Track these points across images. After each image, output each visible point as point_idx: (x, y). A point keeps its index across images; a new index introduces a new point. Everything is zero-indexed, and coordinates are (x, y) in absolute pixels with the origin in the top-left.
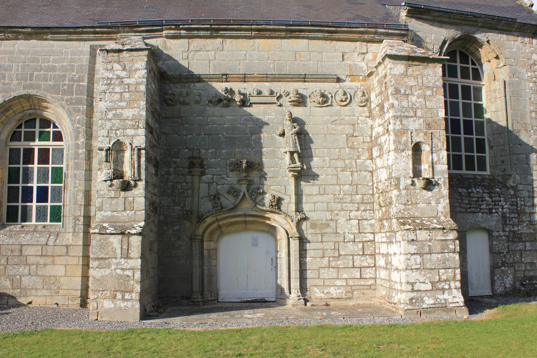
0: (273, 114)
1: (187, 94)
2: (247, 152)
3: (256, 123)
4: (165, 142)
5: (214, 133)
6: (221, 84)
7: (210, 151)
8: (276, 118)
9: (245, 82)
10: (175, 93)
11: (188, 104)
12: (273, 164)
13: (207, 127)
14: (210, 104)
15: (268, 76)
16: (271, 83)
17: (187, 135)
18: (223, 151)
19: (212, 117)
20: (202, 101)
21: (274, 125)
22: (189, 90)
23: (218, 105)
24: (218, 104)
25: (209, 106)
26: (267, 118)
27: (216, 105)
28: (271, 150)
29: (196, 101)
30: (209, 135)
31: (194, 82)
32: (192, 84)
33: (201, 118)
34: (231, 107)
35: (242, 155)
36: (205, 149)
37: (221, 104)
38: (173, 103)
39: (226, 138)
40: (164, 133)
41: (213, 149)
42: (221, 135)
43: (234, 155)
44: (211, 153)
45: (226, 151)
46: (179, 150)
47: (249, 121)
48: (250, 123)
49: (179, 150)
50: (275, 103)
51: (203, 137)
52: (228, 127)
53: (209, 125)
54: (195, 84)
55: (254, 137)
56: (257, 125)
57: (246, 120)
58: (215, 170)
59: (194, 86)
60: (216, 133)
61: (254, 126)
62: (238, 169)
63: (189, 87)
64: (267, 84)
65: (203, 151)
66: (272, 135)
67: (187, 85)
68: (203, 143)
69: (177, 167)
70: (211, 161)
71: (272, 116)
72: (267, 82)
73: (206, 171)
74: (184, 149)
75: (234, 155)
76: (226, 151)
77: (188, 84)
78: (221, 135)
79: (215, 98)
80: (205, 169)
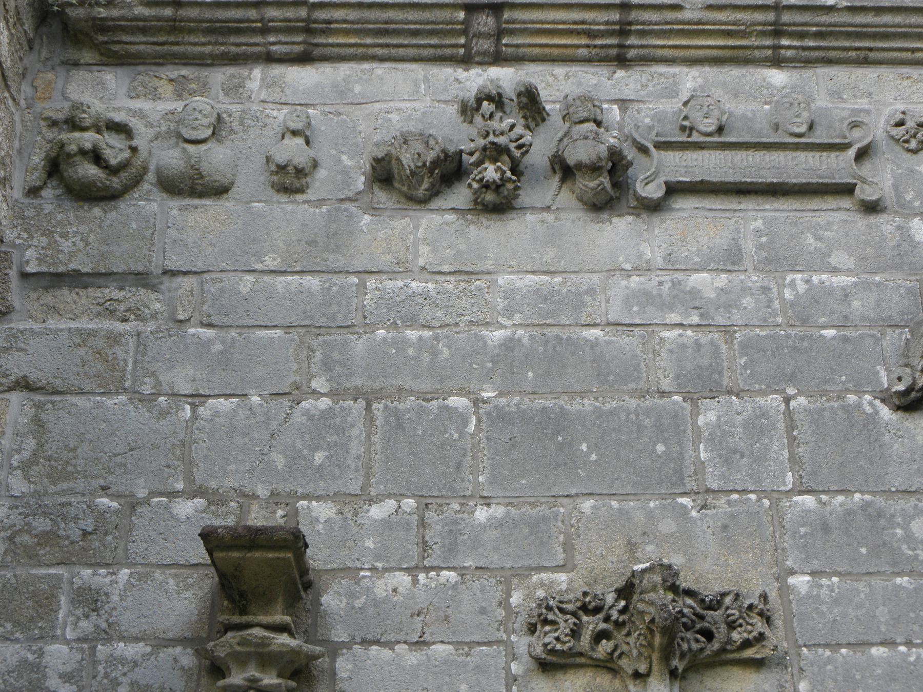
0: (838, 258)
1: (218, 128)
2: (668, 526)
3: (720, 320)
4: (31, 443)
5: (409, 383)
6: (461, 73)
7: (377, 512)
8: (866, 286)
9: (622, 61)
10: (135, 123)
11: (220, 191)
12: (882, 613)
13: (359, 345)
14: (381, 196)
15: (786, 17)
16: (808, 73)
17: (197, 398)
18: (481, 514)
19: (392, 274)
20: (322, 173)
21: (851, 333)
22: (235, 108)
23: (437, 203)
24: (434, 193)
25: (374, 210)
26: (801, 287)
27: (423, 201)
28: (849, 513)
29: (282, 169)
30: (369, 397)
31: (270, 59)
32: (257, 72)
33: (313, 282)
34: (530, 217)
35: (632, 547)
36: (335, 497)
37: (460, 196)
38: (116, 182)
39: (500, 417)
40: (25, 385)
41: (399, 496)
42: (458, 402)
43: (568, 547)
44: (386, 524)
45: (498, 511)
46: (133, 505)
47: (671, 308)
48: (674, 318)
49: (133, 505)
50: (847, 190)
51: (328, 414)
52: (509, 345)
53: (371, 328)
54: (277, 70)
55: (712, 417)
56: (727, 330)
57: (646, 298)
58: (412, 658)
59: (268, 84)
60: (426, 385)
61: (704, 339)
62: (605, 646)
63: (234, 90)
64: (777, 77)
65: (324, 511)
66: (852, 398)
67: (219, 76)
68: (319, 457)
69: (108, 634)
70: (381, 587)
71: (835, 271)
72: (777, 62)
73: (343, 666)
74: (172, 495)
75: (568, 547)
76: (498, 511)
77: (231, 70)
78: (458, 402)
79: (419, 147)
80: (335, 650)
